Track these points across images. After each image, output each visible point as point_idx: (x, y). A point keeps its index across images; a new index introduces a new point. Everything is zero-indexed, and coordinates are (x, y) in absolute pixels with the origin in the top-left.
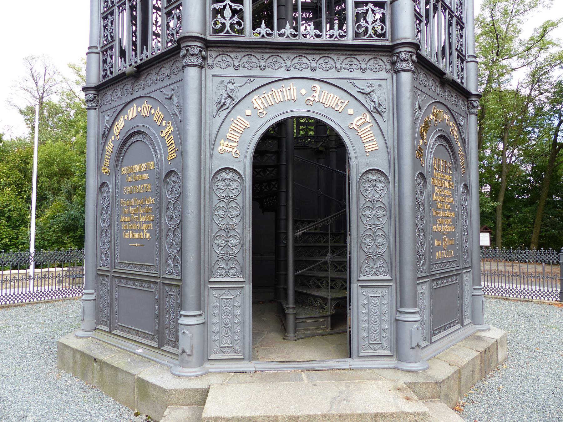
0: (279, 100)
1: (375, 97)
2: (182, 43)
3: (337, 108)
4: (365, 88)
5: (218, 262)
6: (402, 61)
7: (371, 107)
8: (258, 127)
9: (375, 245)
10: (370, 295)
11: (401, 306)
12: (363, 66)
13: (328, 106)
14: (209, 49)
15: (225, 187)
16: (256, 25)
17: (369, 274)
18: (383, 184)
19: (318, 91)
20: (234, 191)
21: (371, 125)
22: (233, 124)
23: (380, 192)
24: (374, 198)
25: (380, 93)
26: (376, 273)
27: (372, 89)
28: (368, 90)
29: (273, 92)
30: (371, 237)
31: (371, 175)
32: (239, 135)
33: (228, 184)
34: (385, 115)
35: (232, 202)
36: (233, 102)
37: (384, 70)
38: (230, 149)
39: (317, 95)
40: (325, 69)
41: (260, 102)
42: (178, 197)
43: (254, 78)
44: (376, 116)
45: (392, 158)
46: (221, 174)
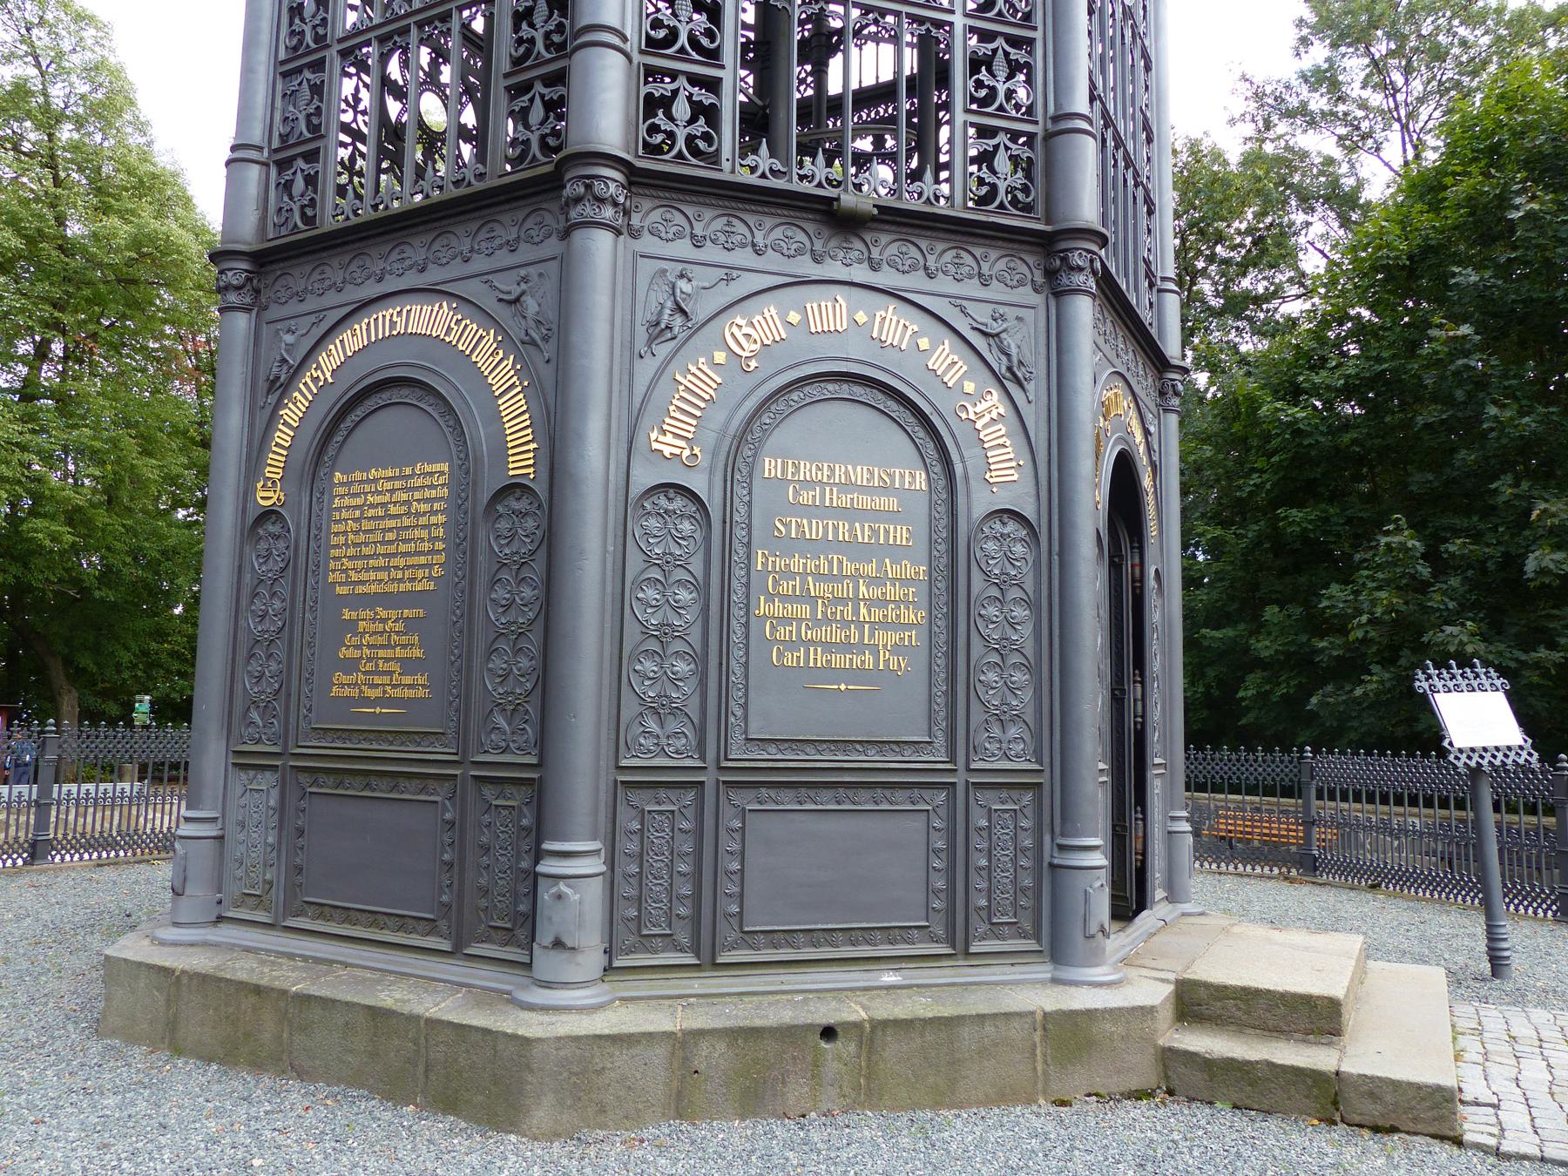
1: (1010, 342)
2: (567, 170)
7: (1000, 366)
11: (1063, 835)
16: (748, 149)
20: (685, 543)
25: (1019, 336)
27: (1005, 326)
34: (1030, 387)
43: (739, 272)
44: (1010, 386)
46: (654, 498)
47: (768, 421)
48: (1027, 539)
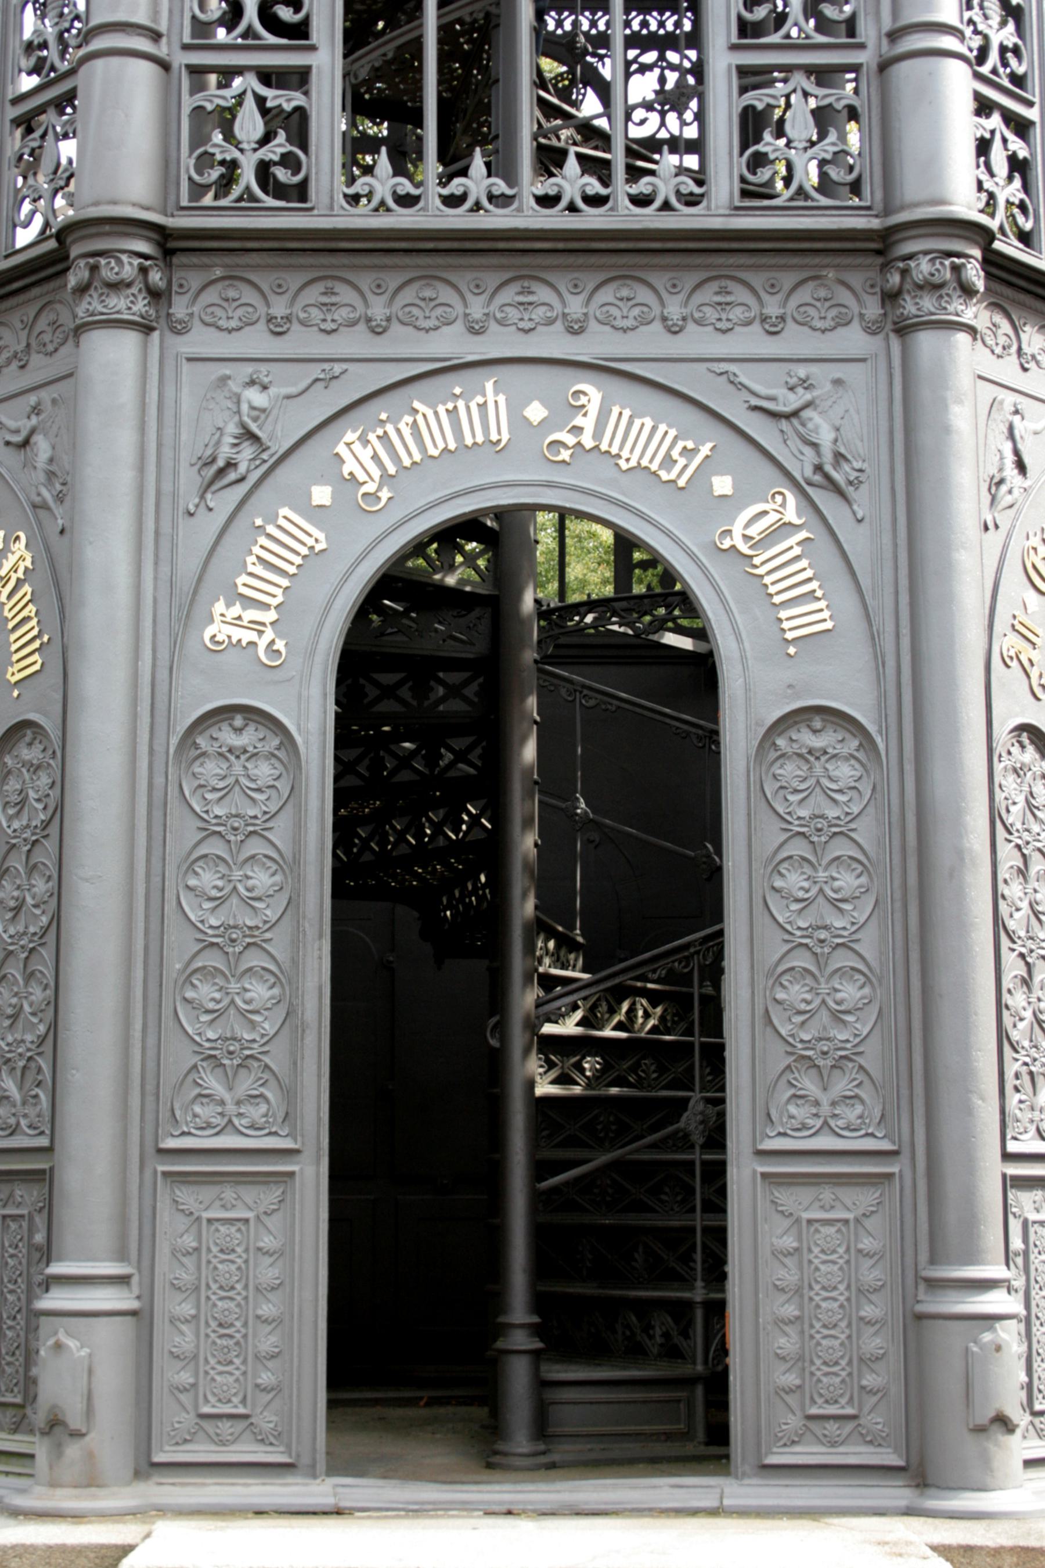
0: (441, 445)
2: (74, 242)
3: (669, 471)
4: (781, 392)
6: (920, 287)
7: (802, 468)
8: (359, 548)
9: (824, 1013)
10: (806, 1215)
12: (773, 309)
13: (633, 463)
14: (176, 260)
15: (230, 780)
17: (804, 1127)
18: (857, 766)
19: (593, 409)
21: (803, 534)
22: (263, 540)
24: (821, 823)
25: (839, 410)
27: (808, 397)
28: (791, 401)
29: (420, 418)
30: (809, 980)
32: (285, 582)
33: (238, 769)
34: (861, 497)
36: (265, 456)
37: (856, 325)
38: (250, 636)
39: (588, 423)
40: (619, 323)
41: (365, 454)
42: (46, 824)
43: (345, 366)
45: (891, 662)
48: (860, 755)
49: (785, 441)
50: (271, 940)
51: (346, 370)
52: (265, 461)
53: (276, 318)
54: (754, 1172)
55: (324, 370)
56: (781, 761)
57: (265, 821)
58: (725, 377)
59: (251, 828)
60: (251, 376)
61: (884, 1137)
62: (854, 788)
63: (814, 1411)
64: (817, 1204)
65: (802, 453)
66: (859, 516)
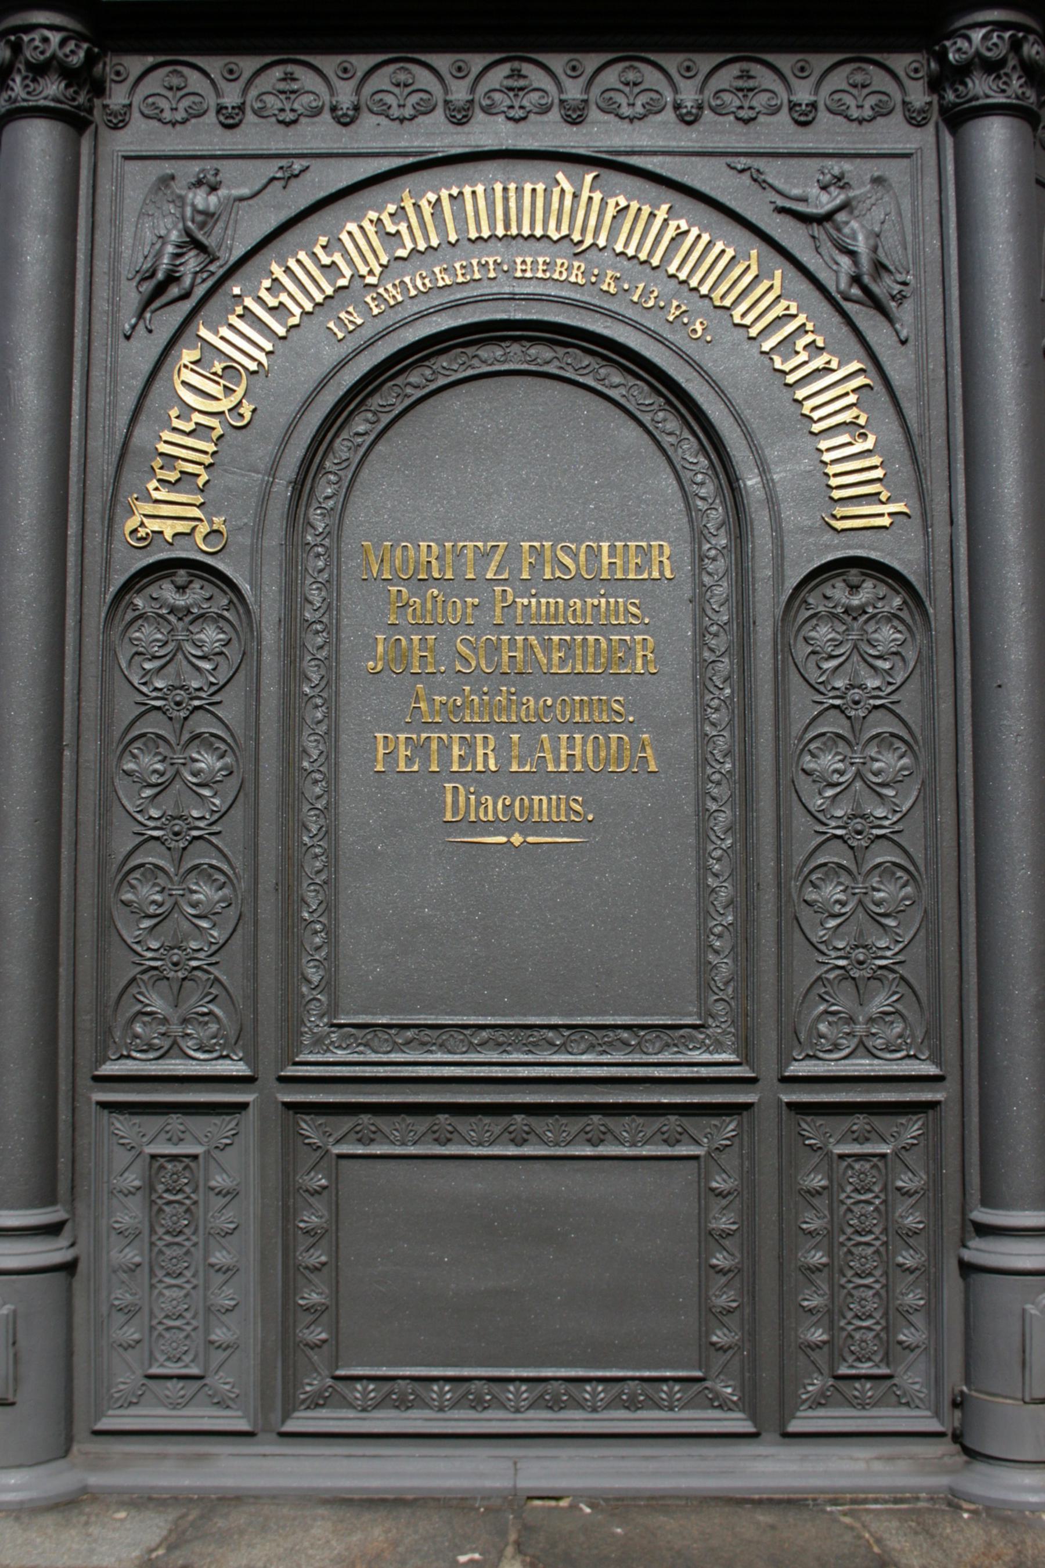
4: (814, 191)
5: (133, 990)
9: (861, 914)
10: (839, 1150)
15: (170, 647)
17: (836, 1047)
18: (901, 627)
23: (887, 665)
24: (856, 694)
25: (878, 214)
26: (870, 1043)
27: (841, 198)
28: (824, 202)
31: (840, 584)
34: (905, 314)
35: (200, 714)
36: (212, 268)
40: (626, 111)
43: (305, 163)
46: (153, 591)
47: (361, 429)
48: (904, 615)
49: (817, 248)
50: (220, 833)
51: (308, 168)
52: (213, 274)
53: (226, 108)
54: (780, 1100)
55: (281, 168)
56: (814, 621)
57: (212, 695)
58: (748, 173)
59: (197, 703)
60: (199, 173)
61: (240, 1060)
62: (221, 653)
63: (155, 1370)
64: (164, 1136)
65: (837, 264)
66: (903, 338)
